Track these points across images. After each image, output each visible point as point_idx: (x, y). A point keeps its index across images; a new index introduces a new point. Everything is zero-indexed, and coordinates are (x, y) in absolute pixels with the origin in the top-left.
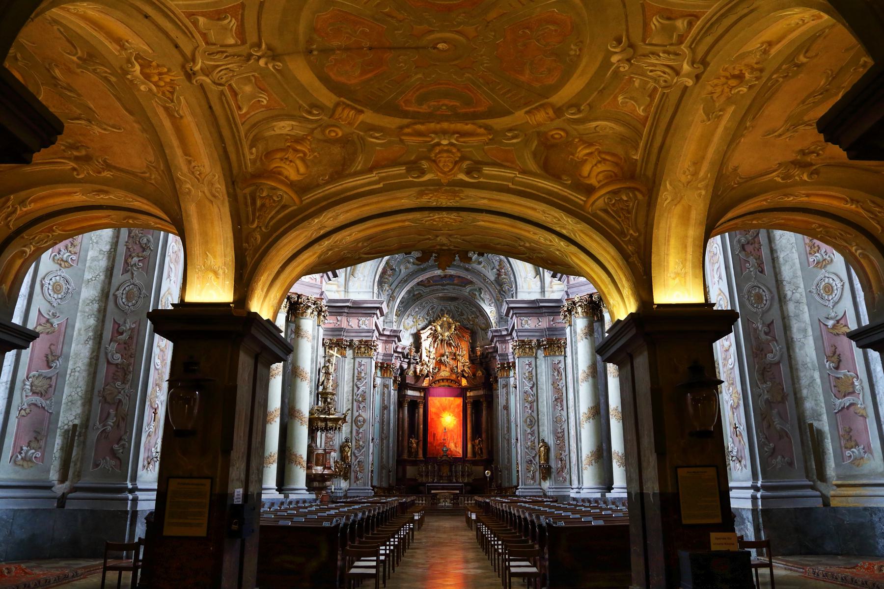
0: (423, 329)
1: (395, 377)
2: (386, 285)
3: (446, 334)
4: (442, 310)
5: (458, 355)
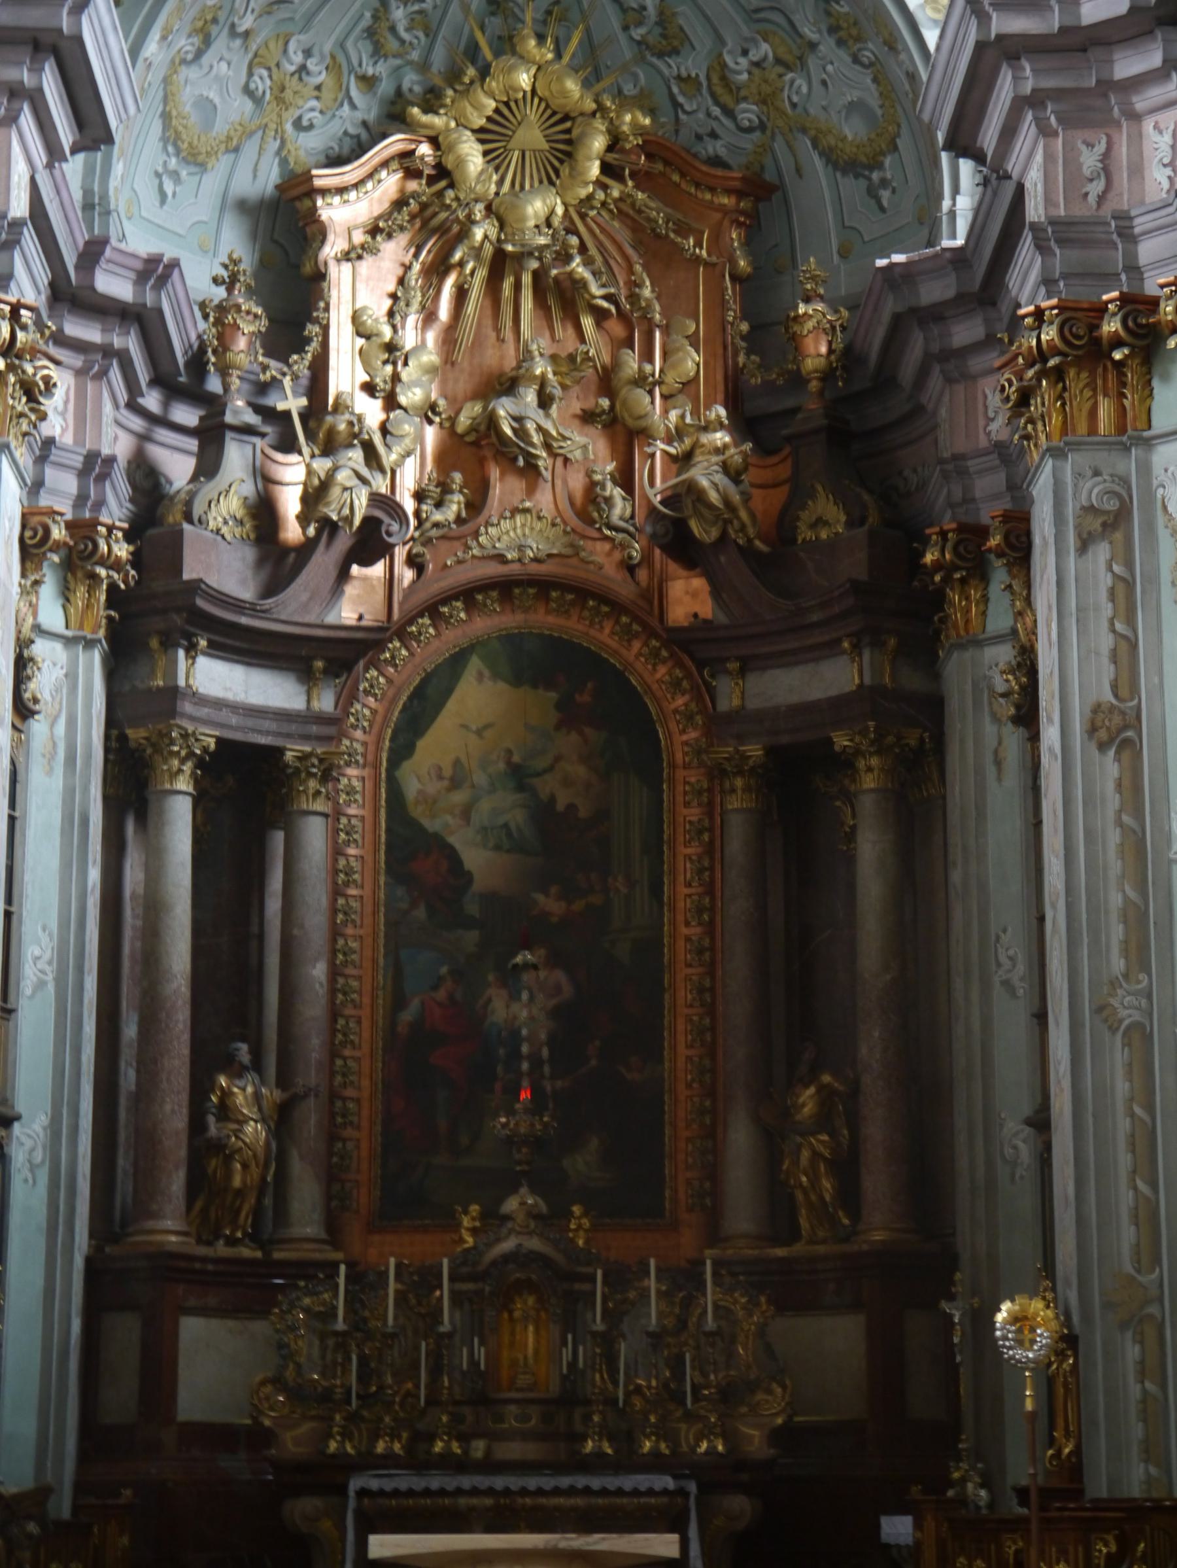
3: (536, 207)
5: (641, 381)
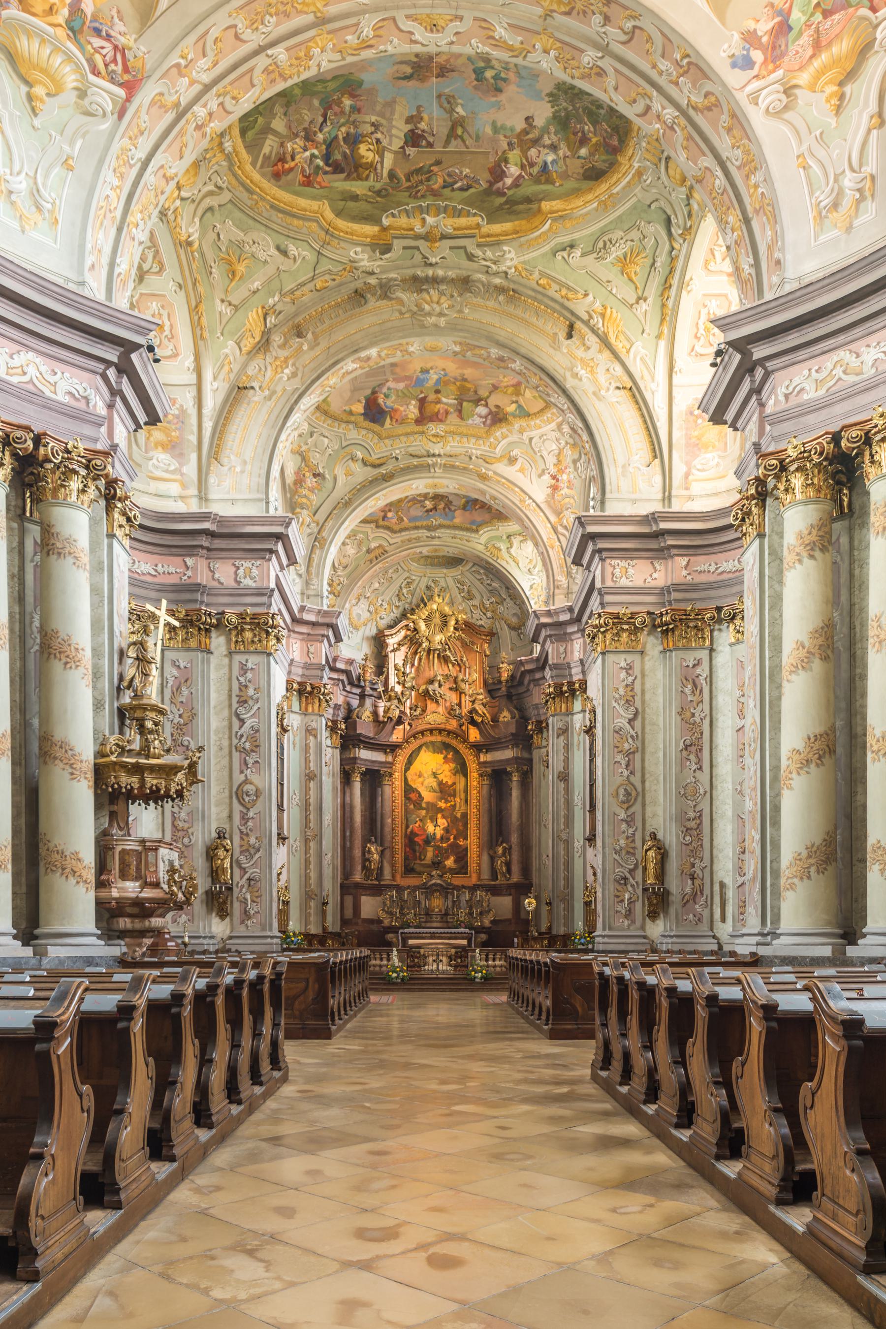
0: (390, 627)
1: (335, 722)
2: (305, 512)
4: (428, 588)
